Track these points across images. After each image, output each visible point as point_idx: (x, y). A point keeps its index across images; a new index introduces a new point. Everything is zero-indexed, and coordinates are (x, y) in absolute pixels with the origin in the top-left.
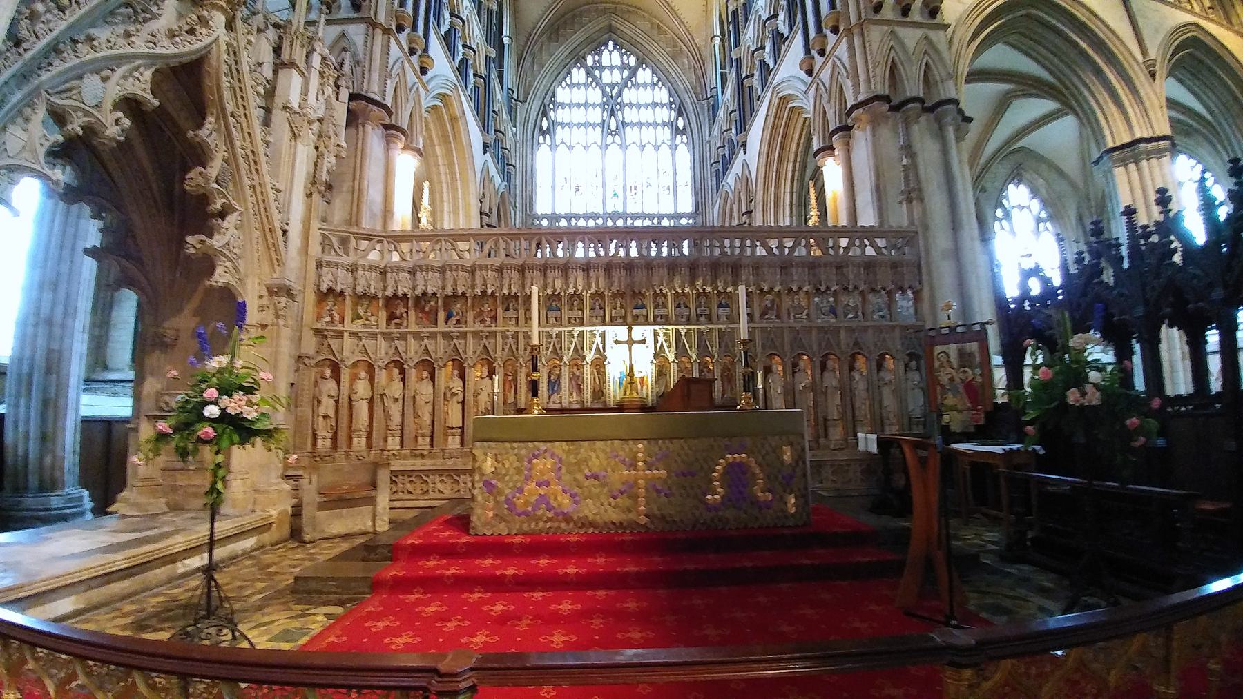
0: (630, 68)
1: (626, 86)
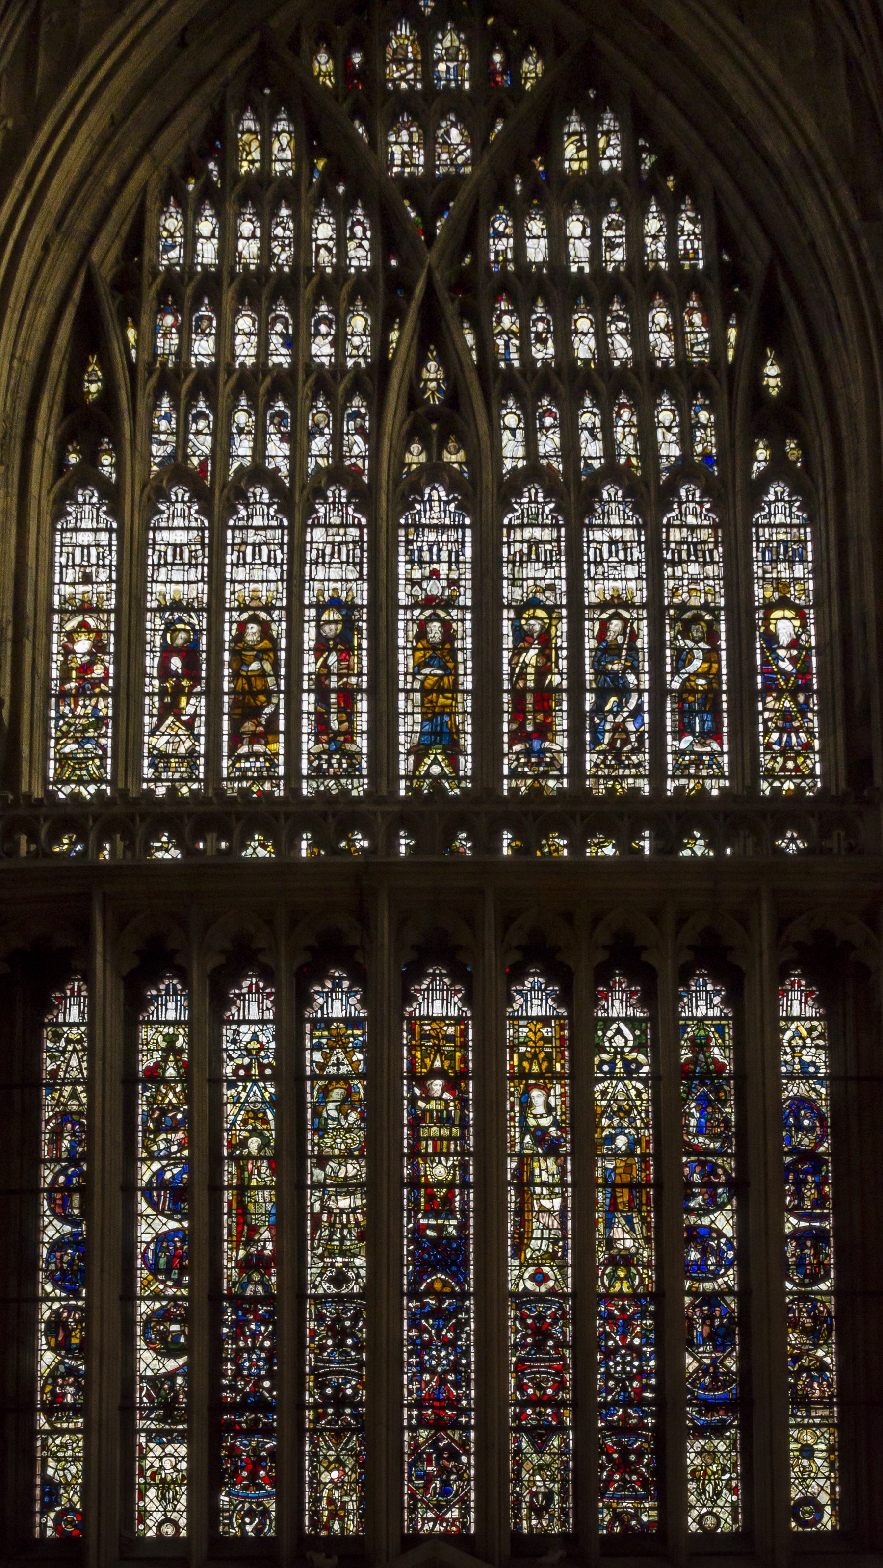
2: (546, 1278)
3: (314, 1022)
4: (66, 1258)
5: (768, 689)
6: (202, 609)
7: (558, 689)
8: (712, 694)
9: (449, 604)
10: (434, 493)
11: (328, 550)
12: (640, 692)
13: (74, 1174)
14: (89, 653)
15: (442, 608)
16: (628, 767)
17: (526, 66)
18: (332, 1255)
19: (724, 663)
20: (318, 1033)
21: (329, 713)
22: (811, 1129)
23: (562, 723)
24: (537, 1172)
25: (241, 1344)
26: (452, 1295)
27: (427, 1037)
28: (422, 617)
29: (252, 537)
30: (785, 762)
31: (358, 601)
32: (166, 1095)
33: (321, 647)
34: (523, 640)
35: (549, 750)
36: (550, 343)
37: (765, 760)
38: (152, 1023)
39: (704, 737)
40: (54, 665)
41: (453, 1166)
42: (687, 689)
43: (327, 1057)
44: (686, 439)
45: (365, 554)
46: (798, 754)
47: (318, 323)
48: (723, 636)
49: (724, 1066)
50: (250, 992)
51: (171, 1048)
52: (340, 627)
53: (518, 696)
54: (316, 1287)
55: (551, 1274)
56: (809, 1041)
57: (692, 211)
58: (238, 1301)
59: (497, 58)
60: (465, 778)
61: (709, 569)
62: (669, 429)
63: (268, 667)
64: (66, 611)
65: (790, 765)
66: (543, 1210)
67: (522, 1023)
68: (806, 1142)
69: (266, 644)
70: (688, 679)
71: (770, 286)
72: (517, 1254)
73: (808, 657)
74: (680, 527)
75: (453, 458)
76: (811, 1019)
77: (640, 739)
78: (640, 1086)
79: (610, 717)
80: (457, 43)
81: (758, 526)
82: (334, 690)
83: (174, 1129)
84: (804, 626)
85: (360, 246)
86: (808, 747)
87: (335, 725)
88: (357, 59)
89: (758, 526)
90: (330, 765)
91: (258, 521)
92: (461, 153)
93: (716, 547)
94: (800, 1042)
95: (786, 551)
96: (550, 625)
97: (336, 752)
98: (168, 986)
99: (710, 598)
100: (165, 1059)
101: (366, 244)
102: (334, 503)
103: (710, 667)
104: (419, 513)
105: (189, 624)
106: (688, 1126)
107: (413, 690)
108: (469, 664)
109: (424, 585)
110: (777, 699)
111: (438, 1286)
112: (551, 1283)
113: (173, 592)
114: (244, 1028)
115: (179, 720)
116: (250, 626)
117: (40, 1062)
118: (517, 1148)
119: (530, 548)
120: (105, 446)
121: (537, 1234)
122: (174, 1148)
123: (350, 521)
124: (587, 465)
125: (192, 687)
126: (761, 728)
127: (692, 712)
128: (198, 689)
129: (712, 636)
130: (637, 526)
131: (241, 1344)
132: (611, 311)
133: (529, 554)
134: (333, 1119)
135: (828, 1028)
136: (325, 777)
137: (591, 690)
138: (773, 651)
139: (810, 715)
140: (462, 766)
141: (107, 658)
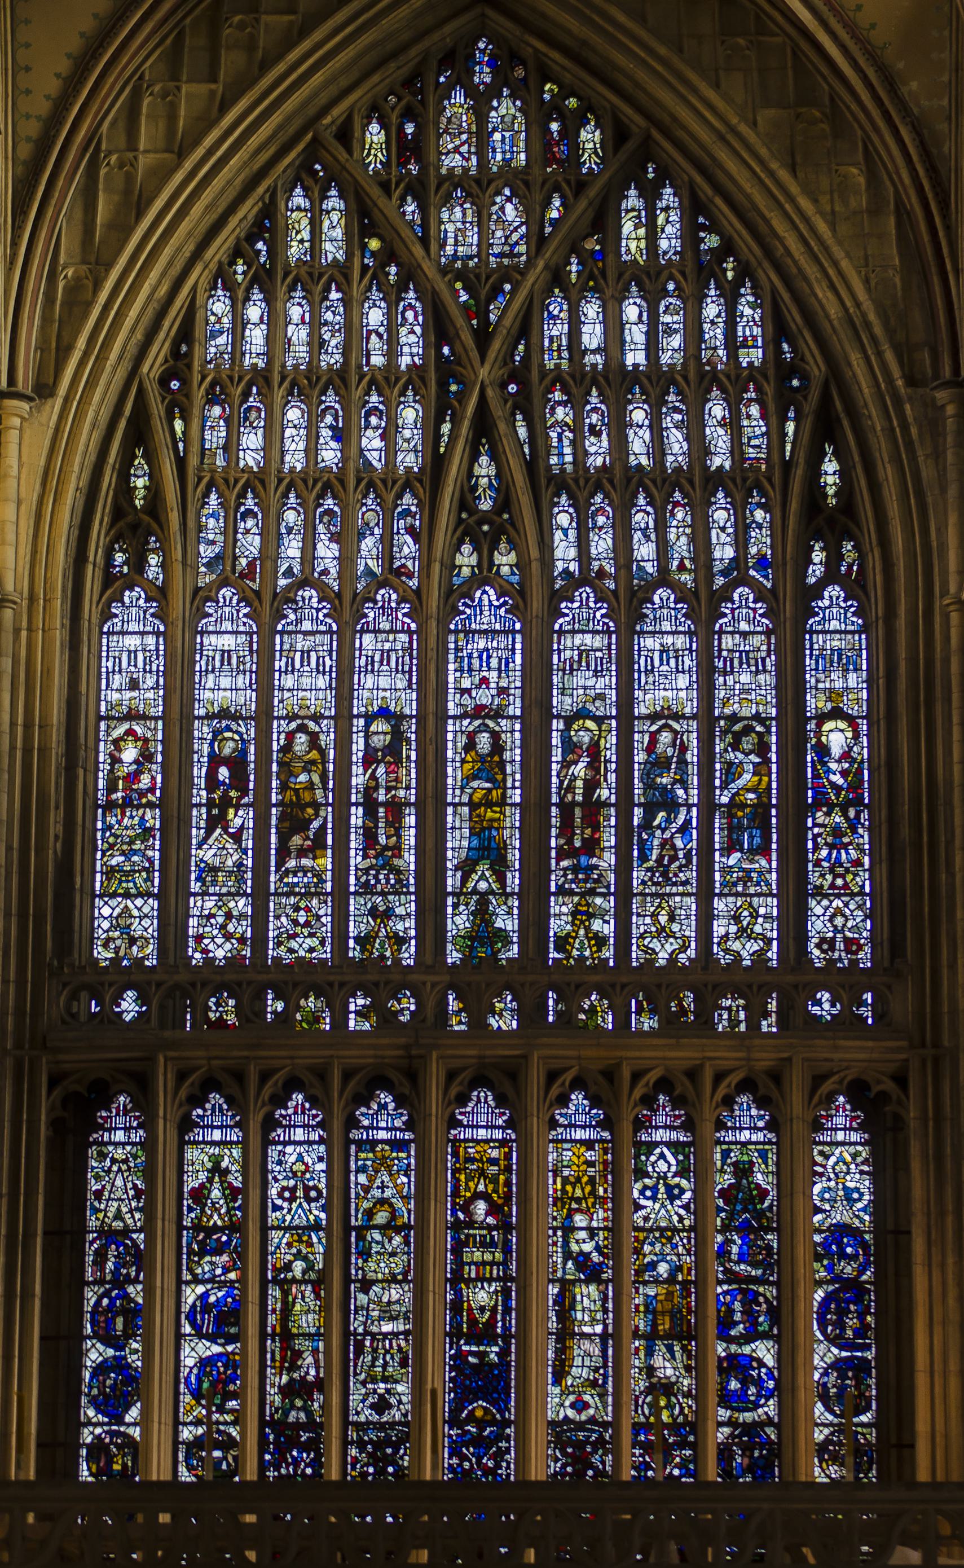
0: (580, 186)
1: (557, 278)
2: (586, 1406)
3: (360, 1144)
4: (109, 1382)
5: (817, 805)
6: (251, 718)
7: (606, 804)
8: (761, 811)
9: (498, 714)
10: (485, 596)
11: (377, 658)
12: (689, 807)
13: (118, 1297)
14: (136, 762)
15: (491, 718)
16: (675, 884)
17: (584, 135)
18: (374, 1380)
19: (774, 776)
20: (363, 1155)
21: (377, 827)
22: (854, 1257)
23: (609, 839)
24: (579, 1298)
25: (283, 1471)
26: (493, 1422)
27: (473, 1160)
28: (471, 728)
29: (301, 642)
30: (834, 879)
31: (407, 711)
32: (211, 1216)
33: (370, 759)
34: (573, 752)
35: (596, 867)
36: (604, 436)
37: (814, 878)
38: (198, 1143)
39: (753, 851)
40: (101, 774)
41: (496, 1292)
42: (734, 804)
43: (371, 1180)
44: (741, 541)
45: (415, 662)
46: (847, 870)
47: (368, 414)
48: (774, 748)
49: (766, 1192)
50: (296, 1113)
51: (217, 1170)
52: (388, 737)
53: (566, 809)
54: (358, 1413)
55: (591, 1402)
56: (853, 1166)
57: (753, 294)
59: (554, 126)
60: (512, 894)
61: (761, 677)
62: (723, 529)
63: (316, 778)
64: (113, 718)
65: (839, 882)
66: (584, 1336)
67: (566, 1146)
68: (849, 1270)
69: (314, 755)
70: (737, 794)
71: (826, 398)
72: (557, 1381)
73: (860, 772)
74: (732, 633)
75: (504, 560)
76: (855, 1144)
77: (688, 855)
78: (682, 1212)
79: (658, 833)
80: (512, 111)
81: (812, 632)
82: (382, 804)
83: (219, 1252)
84: (856, 736)
85: (413, 332)
86: (858, 863)
87: (382, 840)
88: (410, 129)
89: (812, 632)
90: (378, 881)
91: (307, 626)
92: (516, 229)
93: (769, 655)
94: (844, 1168)
95: (840, 659)
96: (600, 736)
97: (383, 868)
98: (214, 1106)
99: (761, 708)
100: (210, 1180)
101: (418, 329)
102: (383, 607)
103: (760, 780)
104: (469, 617)
105: (237, 732)
106: (730, 1253)
107: (461, 804)
108: (518, 777)
109: (474, 693)
110: (828, 814)
111: (479, 1413)
112: (591, 1411)
113: (223, 698)
114: (289, 1149)
115: (227, 832)
116: (298, 735)
117: (85, 1182)
118: (559, 1274)
119: (580, 655)
120: (152, 545)
121: (578, 1361)
122: (219, 1271)
123: (399, 626)
124: (640, 568)
125: (239, 798)
126: (810, 845)
127: (740, 828)
128: (246, 800)
129: (762, 749)
130: (689, 633)
131: (283, 1471)
132: (667, 402)
133: (580, 661)
134: (377, 1243)
135: (872, 1153)
136: (373, 894)
137: (639, 805)
138: (824, 764)
139: (861, 831)
140: (509, 882)
141: (154, 767)
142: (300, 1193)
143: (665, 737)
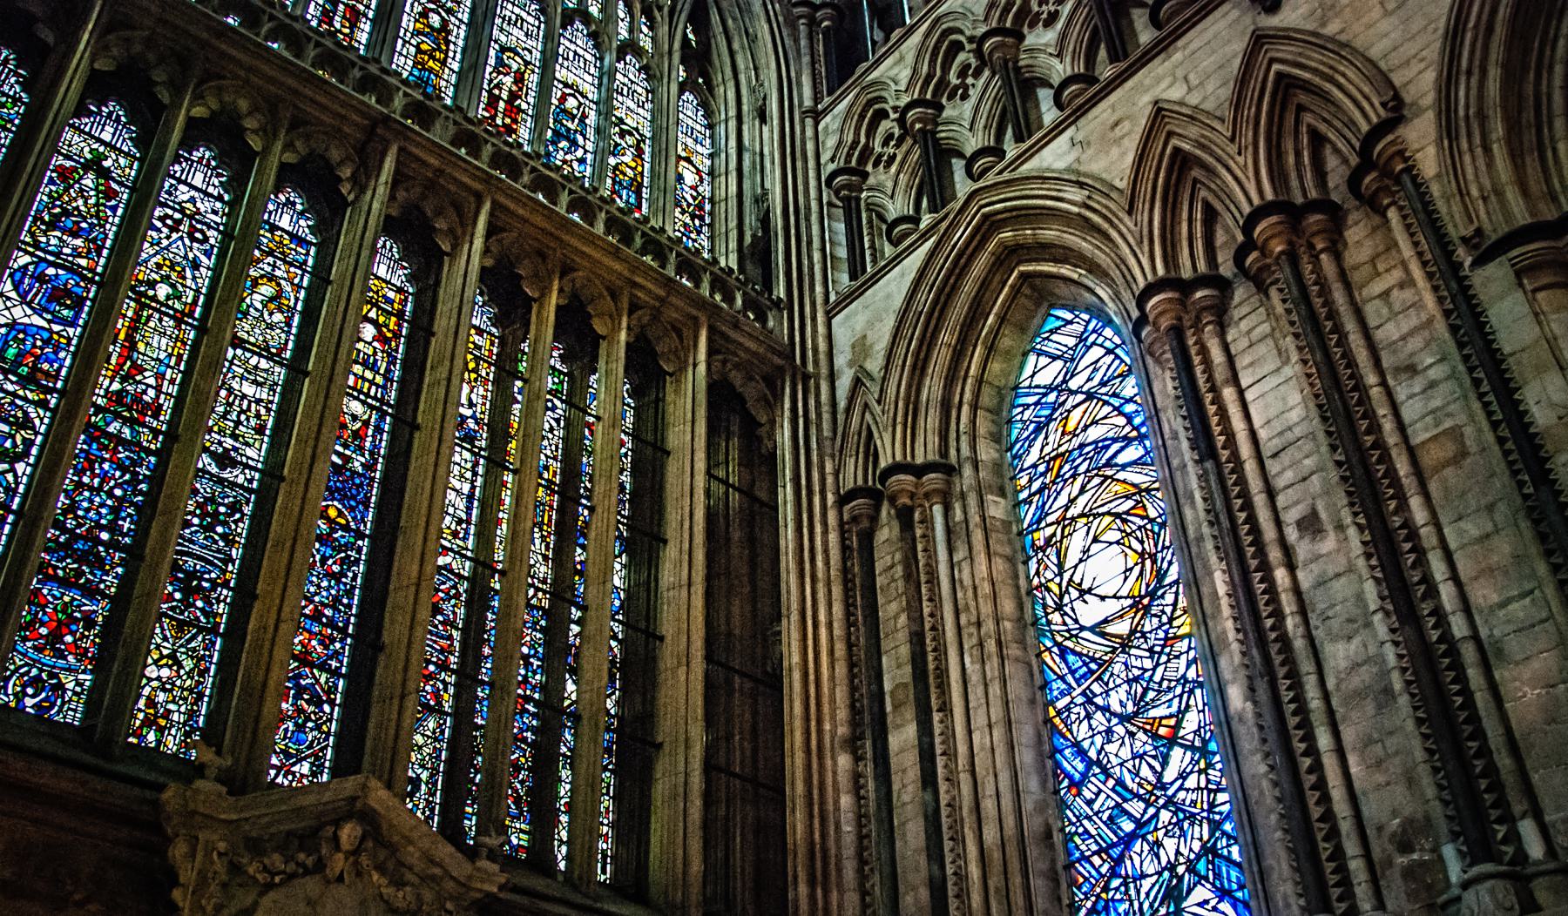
32: (75, 200)
58: (95, 434)
114: (182, 188)
131: (86, 480)
142: (185, 227)
143: (571, 103)
